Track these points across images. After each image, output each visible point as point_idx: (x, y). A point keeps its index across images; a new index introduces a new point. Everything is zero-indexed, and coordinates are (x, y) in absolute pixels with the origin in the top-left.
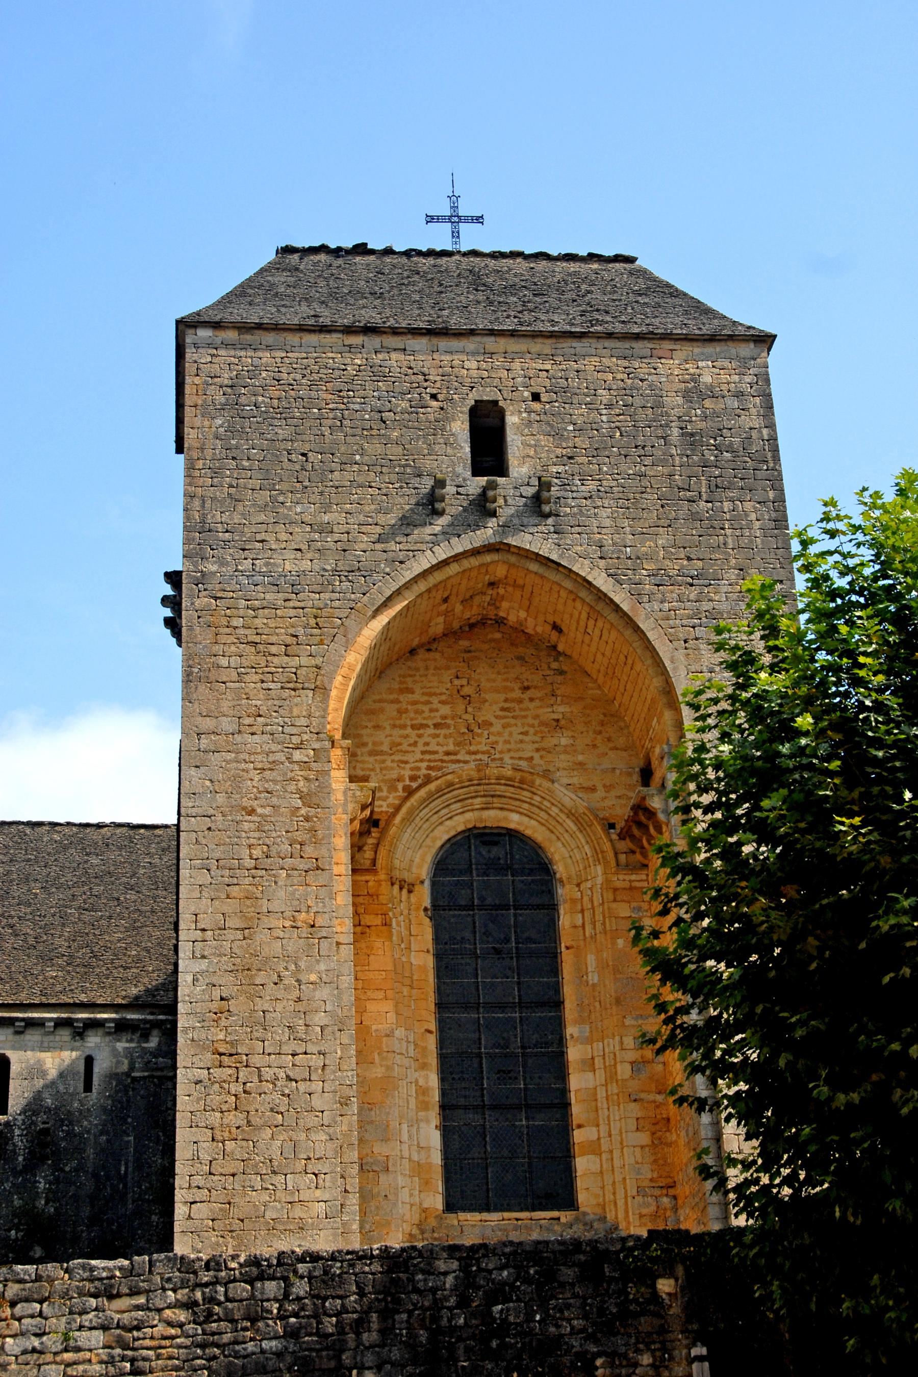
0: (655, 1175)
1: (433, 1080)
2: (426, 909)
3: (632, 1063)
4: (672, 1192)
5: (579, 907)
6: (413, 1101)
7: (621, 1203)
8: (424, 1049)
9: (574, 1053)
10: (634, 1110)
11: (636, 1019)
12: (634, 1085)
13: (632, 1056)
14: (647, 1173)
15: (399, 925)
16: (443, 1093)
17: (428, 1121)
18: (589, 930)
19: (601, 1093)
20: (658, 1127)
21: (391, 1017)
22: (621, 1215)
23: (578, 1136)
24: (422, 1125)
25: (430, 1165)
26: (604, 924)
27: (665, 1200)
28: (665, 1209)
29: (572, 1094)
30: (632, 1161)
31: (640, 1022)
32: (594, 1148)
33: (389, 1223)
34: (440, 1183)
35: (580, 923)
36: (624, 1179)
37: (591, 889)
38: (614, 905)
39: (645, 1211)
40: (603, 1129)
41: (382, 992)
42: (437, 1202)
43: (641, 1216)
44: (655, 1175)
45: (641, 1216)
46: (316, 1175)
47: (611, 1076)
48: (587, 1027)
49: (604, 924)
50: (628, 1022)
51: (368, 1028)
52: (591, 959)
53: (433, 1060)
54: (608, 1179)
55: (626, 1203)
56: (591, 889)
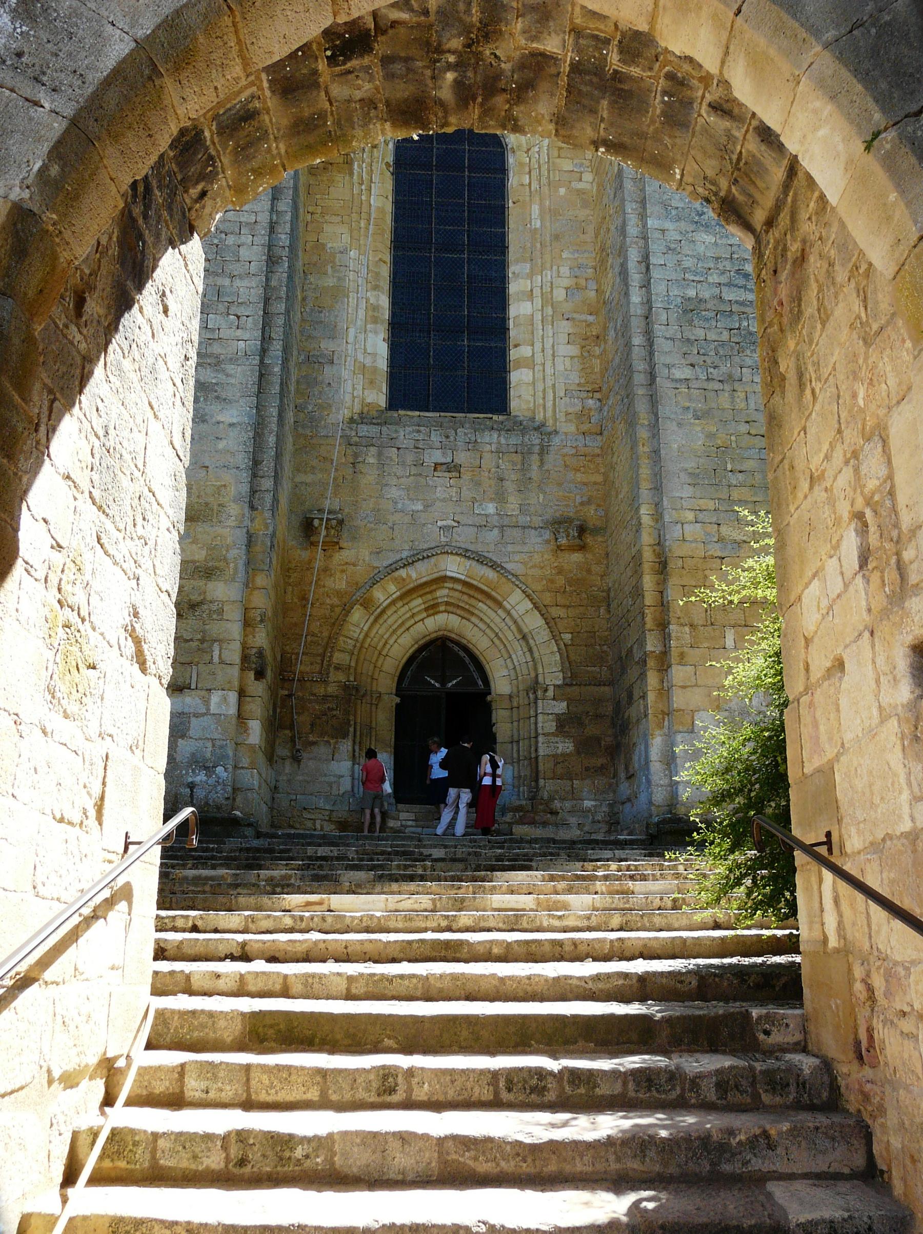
0: (583, 381)
1: (384, 301)
2: (387, 164)
3: (567, 289)
4: (597, 395)
5: (527, 170)
6: (361, 313)
7: (550, 404)
8: (377, 274)
9: (514, 288)
10: (565, 327)
11: (573, 253)
12: (567, 307)
13: (566, 282)
14: (575, 378)
15: (360, 167)
16: (393, 314)
17: (376, 333)
18: (535, 185)
19: (538, 316)
20: (587, 342)
21: (346, 238)
22: (549, 413)
23: (513, 354)
24: (370, 335)
25: (375, 370)
26: (549, 177)
27: (590, 401)
28: (590, 409)
29: (511, 321)
30: (561, 368)
31: (576, 255)
32: (530, 363)
33: (330, 406)
34: (384, 385)
35: (528, 181)
36: (554, 385)
37: (538, 152)
38: (558, 160)
39: (570, 410)
40: (538, 346)
41: (339, 218)
42: (381, 400)
43: (567, 414)
44: (583, 381)
45: (567, 414)
46: (238, 317)
47: (547, 299)
48: (528, 265)
49: (549, 177)
50: (564, 255)
51: (324, 246)
52: (535, 209)
53: (385, 284)
54: (540, 386)
55: (554, 404)
56: (538, 152)
